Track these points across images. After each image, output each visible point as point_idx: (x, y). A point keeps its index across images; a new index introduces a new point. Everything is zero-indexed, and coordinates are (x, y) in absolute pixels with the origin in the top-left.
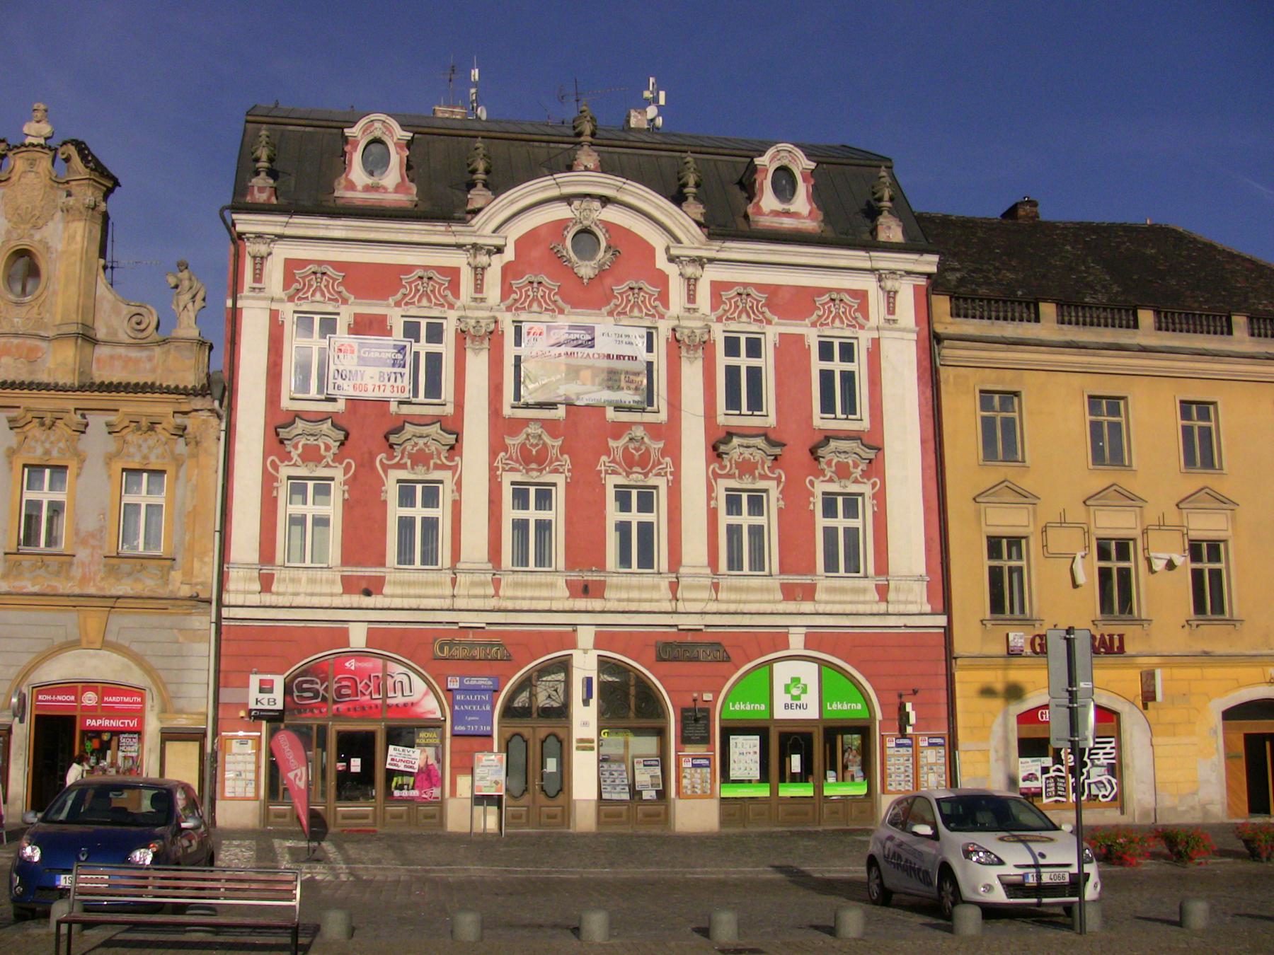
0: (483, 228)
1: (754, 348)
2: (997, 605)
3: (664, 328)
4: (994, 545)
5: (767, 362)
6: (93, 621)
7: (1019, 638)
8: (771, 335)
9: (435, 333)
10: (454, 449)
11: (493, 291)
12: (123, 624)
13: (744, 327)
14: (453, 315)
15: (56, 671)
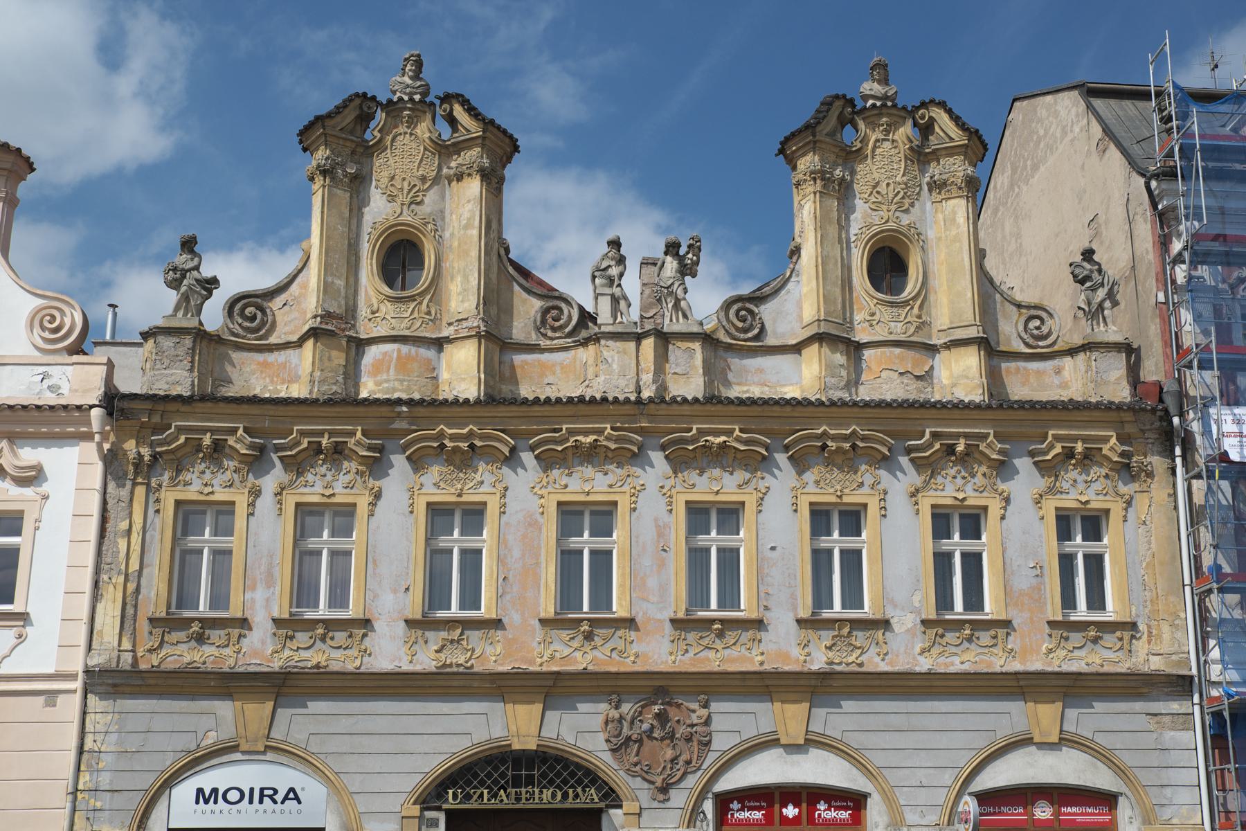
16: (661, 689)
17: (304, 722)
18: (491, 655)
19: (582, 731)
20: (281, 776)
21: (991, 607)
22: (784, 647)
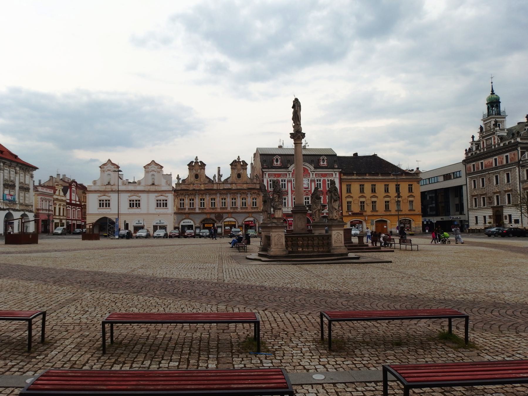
0: (290, 169)
1: (320, 181)
2: (348, 209)
3: (310, 179)
4: (348, 202)
5: (321, 182)
6: (250, 215)
7: (350, 213)
8: (322, 179)
9: (285, 181)
10: (288, 194)
11: (291, 176)
12: (254, 215)
13: (319, 178)
14: (286, 179)
15: (247, 220)
16: (219, 213)
17: (191, 216)
18: (205, 211)
19: (213, 217)
20: (190, 221)
21: (247, 206)
22: (229, 209)
